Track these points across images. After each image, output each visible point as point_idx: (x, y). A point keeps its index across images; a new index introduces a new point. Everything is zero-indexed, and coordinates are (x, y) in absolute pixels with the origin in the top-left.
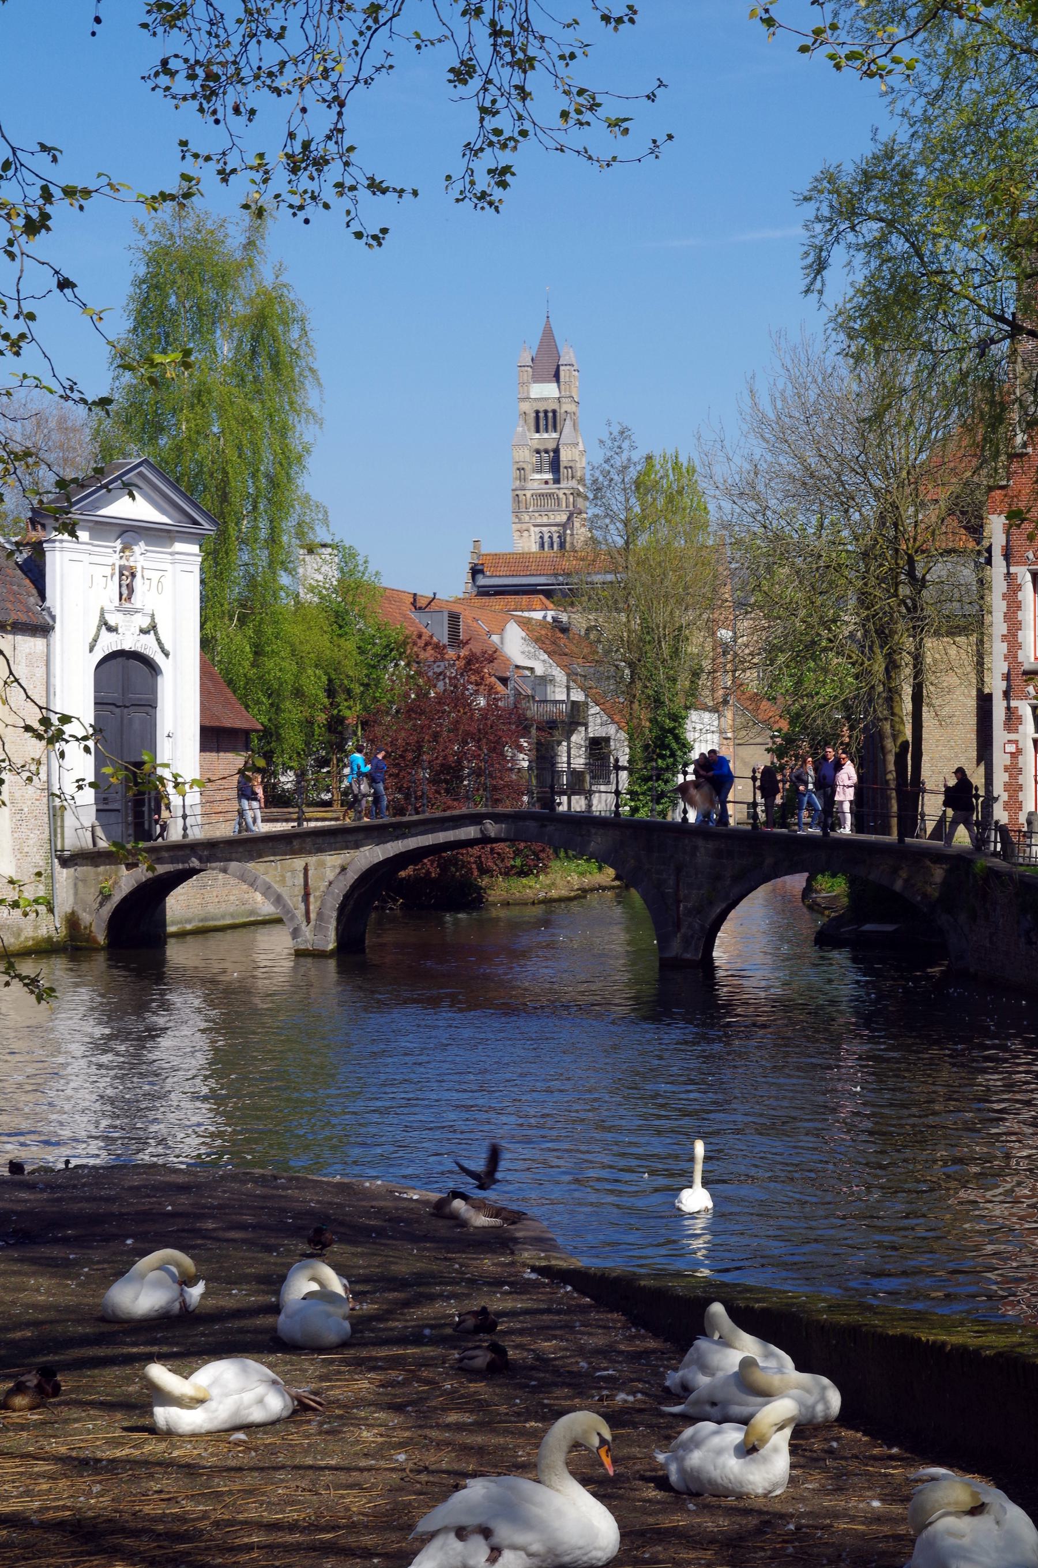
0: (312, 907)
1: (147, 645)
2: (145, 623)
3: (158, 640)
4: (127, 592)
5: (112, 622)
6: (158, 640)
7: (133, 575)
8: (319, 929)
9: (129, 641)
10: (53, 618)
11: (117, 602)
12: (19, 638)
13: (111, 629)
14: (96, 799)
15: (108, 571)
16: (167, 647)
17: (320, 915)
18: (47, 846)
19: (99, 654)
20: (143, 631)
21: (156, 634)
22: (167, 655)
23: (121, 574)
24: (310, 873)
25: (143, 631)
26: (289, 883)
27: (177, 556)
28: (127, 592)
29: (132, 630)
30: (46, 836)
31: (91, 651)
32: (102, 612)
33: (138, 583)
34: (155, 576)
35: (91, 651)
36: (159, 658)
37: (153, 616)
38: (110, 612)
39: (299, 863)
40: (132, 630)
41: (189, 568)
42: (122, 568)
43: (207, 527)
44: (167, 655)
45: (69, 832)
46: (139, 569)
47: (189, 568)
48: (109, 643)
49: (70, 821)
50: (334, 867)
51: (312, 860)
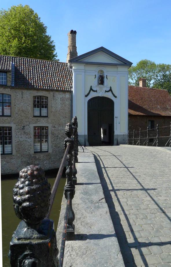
1: (109, 95)
2: (108, 89)
9: (101, 93)
16: (116, 95)
19: (90, 97)
20: (106, 91)
21: (112, 92)
22: (116, 97)
25: (106, 91)
27: (118, 72)
31: (86, 96)
32: (91, 87)
35: (86, 96)
37: (111, 87)
44: (116, 97)
48: (93, 95)
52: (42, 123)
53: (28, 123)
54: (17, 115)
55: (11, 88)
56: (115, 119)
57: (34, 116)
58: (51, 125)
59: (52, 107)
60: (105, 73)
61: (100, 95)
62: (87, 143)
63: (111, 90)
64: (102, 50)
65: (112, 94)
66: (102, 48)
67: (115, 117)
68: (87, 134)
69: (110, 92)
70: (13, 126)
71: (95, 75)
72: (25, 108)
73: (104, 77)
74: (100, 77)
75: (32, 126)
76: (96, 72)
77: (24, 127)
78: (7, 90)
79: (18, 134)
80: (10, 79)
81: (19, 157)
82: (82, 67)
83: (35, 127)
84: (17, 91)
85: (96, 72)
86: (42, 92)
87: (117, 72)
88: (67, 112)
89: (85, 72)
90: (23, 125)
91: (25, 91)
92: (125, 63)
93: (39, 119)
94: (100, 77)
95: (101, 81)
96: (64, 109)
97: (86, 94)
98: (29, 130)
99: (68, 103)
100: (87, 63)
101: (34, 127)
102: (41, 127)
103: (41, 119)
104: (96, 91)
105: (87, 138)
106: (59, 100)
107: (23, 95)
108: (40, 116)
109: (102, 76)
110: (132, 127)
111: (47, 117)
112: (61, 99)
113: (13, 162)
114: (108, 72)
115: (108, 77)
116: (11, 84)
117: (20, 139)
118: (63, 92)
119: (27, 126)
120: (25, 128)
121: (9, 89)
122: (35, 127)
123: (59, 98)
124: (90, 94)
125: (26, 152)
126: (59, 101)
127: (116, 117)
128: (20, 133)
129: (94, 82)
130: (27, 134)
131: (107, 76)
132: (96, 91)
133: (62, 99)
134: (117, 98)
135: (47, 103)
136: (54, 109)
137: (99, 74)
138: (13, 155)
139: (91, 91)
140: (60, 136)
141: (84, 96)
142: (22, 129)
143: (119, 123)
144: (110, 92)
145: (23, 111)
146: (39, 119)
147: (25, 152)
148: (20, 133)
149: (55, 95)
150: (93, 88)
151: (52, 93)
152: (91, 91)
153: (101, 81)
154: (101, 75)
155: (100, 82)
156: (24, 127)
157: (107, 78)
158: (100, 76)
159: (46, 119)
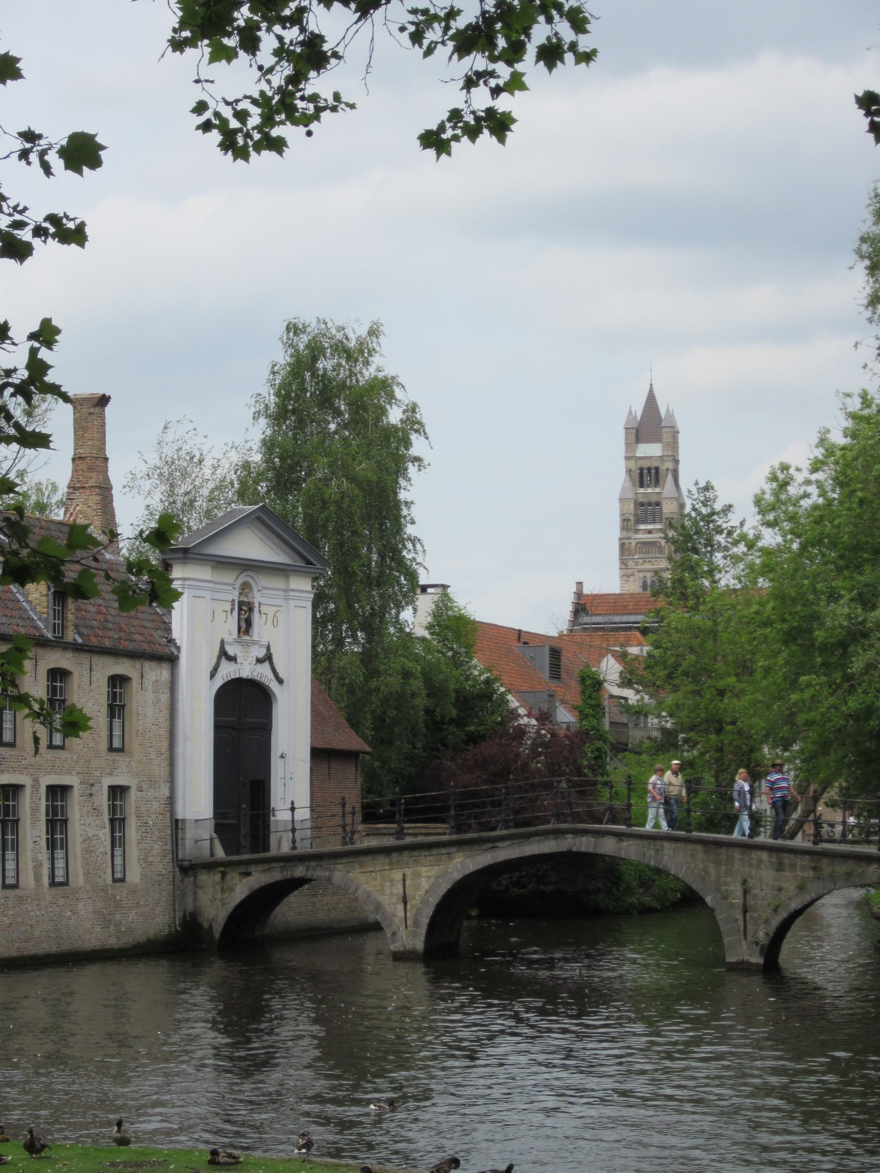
0: (408, 914)
1: (263, 674)
2: (262, 653)
4: (246, 626)
5: (231, 650)
7: (251, 610)
8: (414, 934)
9: (246, 669)
10: (178, 649)
11: (236, 636)
12: (147, 665)
14: (215, 814)
15: (228, 607)
17: (416, 923)
18: (170, 857)
19: (219, 681)
20: (259, 661)
22: (280, 681)
23: (240, 609)
24: (407, 883)
25: (259, 661)
26: (388, 892)
27: (291, 593)
28: (246, 626)
29: (250, 659)
30: (169, 847)
31: (213, 675)
32: (222, 642)
33: (256, 617)
34: (271, 611)
35: (213, 675)
36: (274, 686)
37: (268, 648)
38: (230, 644)
39: (397, 875)
41: (303, 604)
42: (241, 604)
43: (319, 566)
44: (280, 681)
45: (189, 843)
46: (256, 605)
47: (303, 604)
48: (228, 672)
49: (190, 834)
50: (429, 877)
51: (408, 872)
54: (82, 746)
55: (76, 648)
63: (268, 658)
69: (267, 663)
71: (233, 601)
77: (92, 785)
82: (203, 573)
87: (285, 591)
90: (91, 782)
92: (309, 562)
100: (219, 562)
104: (232, 659)
111: (121, 750)
114: (267, 594)
115: (263, 608)
121: (71, 654)
127: (282, 757)
129: (227, 626)
131: (260, 604)
132: (232, 659)
139: (224, 661)
140: (151, 823)
143: (291, 778)
144: (267, 663)
146: (117, 758)
151: (138, 664)
155: (243, 625)
156: (92, 785)
157: (260, 612)
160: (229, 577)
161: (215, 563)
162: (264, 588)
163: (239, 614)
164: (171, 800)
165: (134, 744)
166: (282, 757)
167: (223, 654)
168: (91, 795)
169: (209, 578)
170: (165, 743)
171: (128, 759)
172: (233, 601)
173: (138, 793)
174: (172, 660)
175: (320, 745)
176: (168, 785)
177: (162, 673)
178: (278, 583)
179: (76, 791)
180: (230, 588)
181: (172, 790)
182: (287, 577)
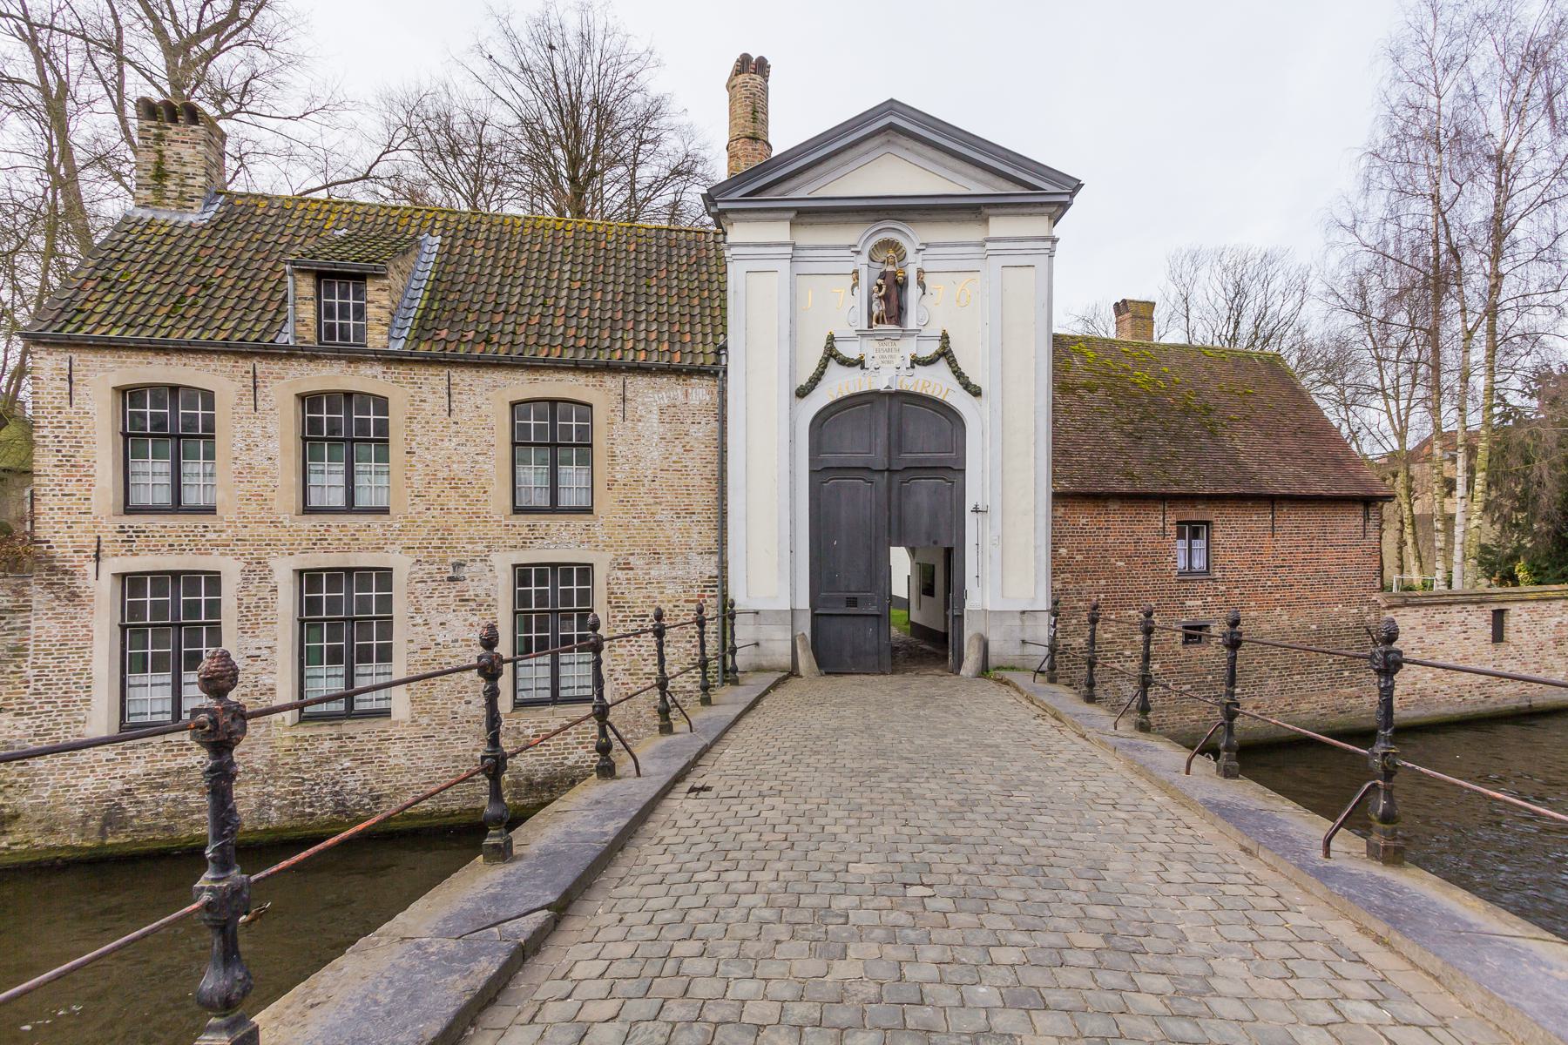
1: (937, 383)
3: (959, 374)
5: (849, 350)
6: (959, 374)
12: (639, 383)
13: (846, 362)
15: (850, 281)
16: (973, 381)
20: (916, 362)
21: (952, 363)
22: (976, 392)
25: (916, 362)
31: (802, 393)
32: (831, 338)
33: (913, 292)
35: (802, 393)
37: (945, 337)
38: (846, 339)
40: (898, 362)
44: (976, 392)
48: (840, 384)
52: (559, 543)
53: (480, 547)
54: (422, 508)
56: (970, 519)
57: (517, 510)
58: (609, 555)
59: (613, 456)
60: (911, 257)
61: (881, 381)
62: (805, 661)
63: (945, 354)
64: (891, 126)
65: (956, 382)
66: (891, 106)
67: (969, 507)
68: (804, 603)
69: (943, 362)
70: (401, 564)
71: (856, 272)
72: (469, 464)
73: (905, 279)
74: (880, 281)
75: (503, 563)
76: (858, 253)
77: (458, 566)
78: (365, 370)
79: (424, 604)
80: (386, 317)
81: (425, 733)
82: (780, 231)
83: (522, 574)
84: (421, 373)
85: (858, 253)
86: (557, 376)
88: (697, 480)
89: (792, 259)
91: (462, 377)
93: (542, 521)
94: (880, 281)
95: (891, 302)
96: (678, 466)
97: (803, 380)
98: (486, 585)
99: (702, 431)
100: (801, 212)
101: (515, 566)
102: (554, 566)
103: (561, 520)
104: (860, 363)
105: (805, 627)
106: (655, 417)
107: (454, 398)
108: (554, 508)
109: (895, 274)
110: (1079, 557)
112: (662, 411)
113: (392, 762)
115: (927, 279)
116: (391, 338)
117: (433, 631)
118: (673, 379)
119: (479, 564)
120: (465, 572)
121: (378, 369)
122: (522, 574)
123: (655, 409)
124: (825, 379)
125: (468, 703)
126: (652, 425)
127: (976, 510)
128: (435, 601)
130: (473, 605)
131: (921, 272)
132: (860, 363)
133: (670, 414)
134: (982, 400)
135: (586, 432)
136: (627, 467)
137: (878, 268)
138: (397, 723)
139: (833, 363)
141: (785, 393)
142: (451, 579)
144: (943, 362)
145: (454, 483)
147: (464, 706)
148: (435, 601)
149: (628, 395)
150: (841, 347)
151: (612, 383)
152: (833, 363)
153: (891, 302)
154: (890, 268)
158: (883, 275)
159: (578, 522)
160: (856, 235)
161: (792, 215)
162: (927, 245)
163: (870, 293)
164: (721, 579)
165: (605, 503)
166: (976, 510)
167: (832, 353)
168: (451, 579)
169: (786, 238)
170: (703, 499)
171: (583, 524)
172: (856, 272)
173: (619, 573)
174: (715, 372)
175: (1065, 485)
176: (715, 558)
177: (700, 392)
178: (970, 232)
179: (398, 580)
180: (847, 252)
181: (723, 566)
182: (986, 221)
